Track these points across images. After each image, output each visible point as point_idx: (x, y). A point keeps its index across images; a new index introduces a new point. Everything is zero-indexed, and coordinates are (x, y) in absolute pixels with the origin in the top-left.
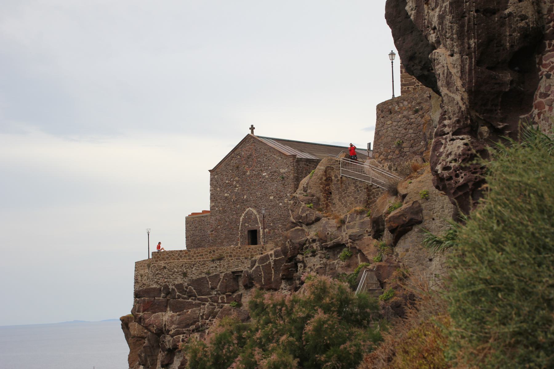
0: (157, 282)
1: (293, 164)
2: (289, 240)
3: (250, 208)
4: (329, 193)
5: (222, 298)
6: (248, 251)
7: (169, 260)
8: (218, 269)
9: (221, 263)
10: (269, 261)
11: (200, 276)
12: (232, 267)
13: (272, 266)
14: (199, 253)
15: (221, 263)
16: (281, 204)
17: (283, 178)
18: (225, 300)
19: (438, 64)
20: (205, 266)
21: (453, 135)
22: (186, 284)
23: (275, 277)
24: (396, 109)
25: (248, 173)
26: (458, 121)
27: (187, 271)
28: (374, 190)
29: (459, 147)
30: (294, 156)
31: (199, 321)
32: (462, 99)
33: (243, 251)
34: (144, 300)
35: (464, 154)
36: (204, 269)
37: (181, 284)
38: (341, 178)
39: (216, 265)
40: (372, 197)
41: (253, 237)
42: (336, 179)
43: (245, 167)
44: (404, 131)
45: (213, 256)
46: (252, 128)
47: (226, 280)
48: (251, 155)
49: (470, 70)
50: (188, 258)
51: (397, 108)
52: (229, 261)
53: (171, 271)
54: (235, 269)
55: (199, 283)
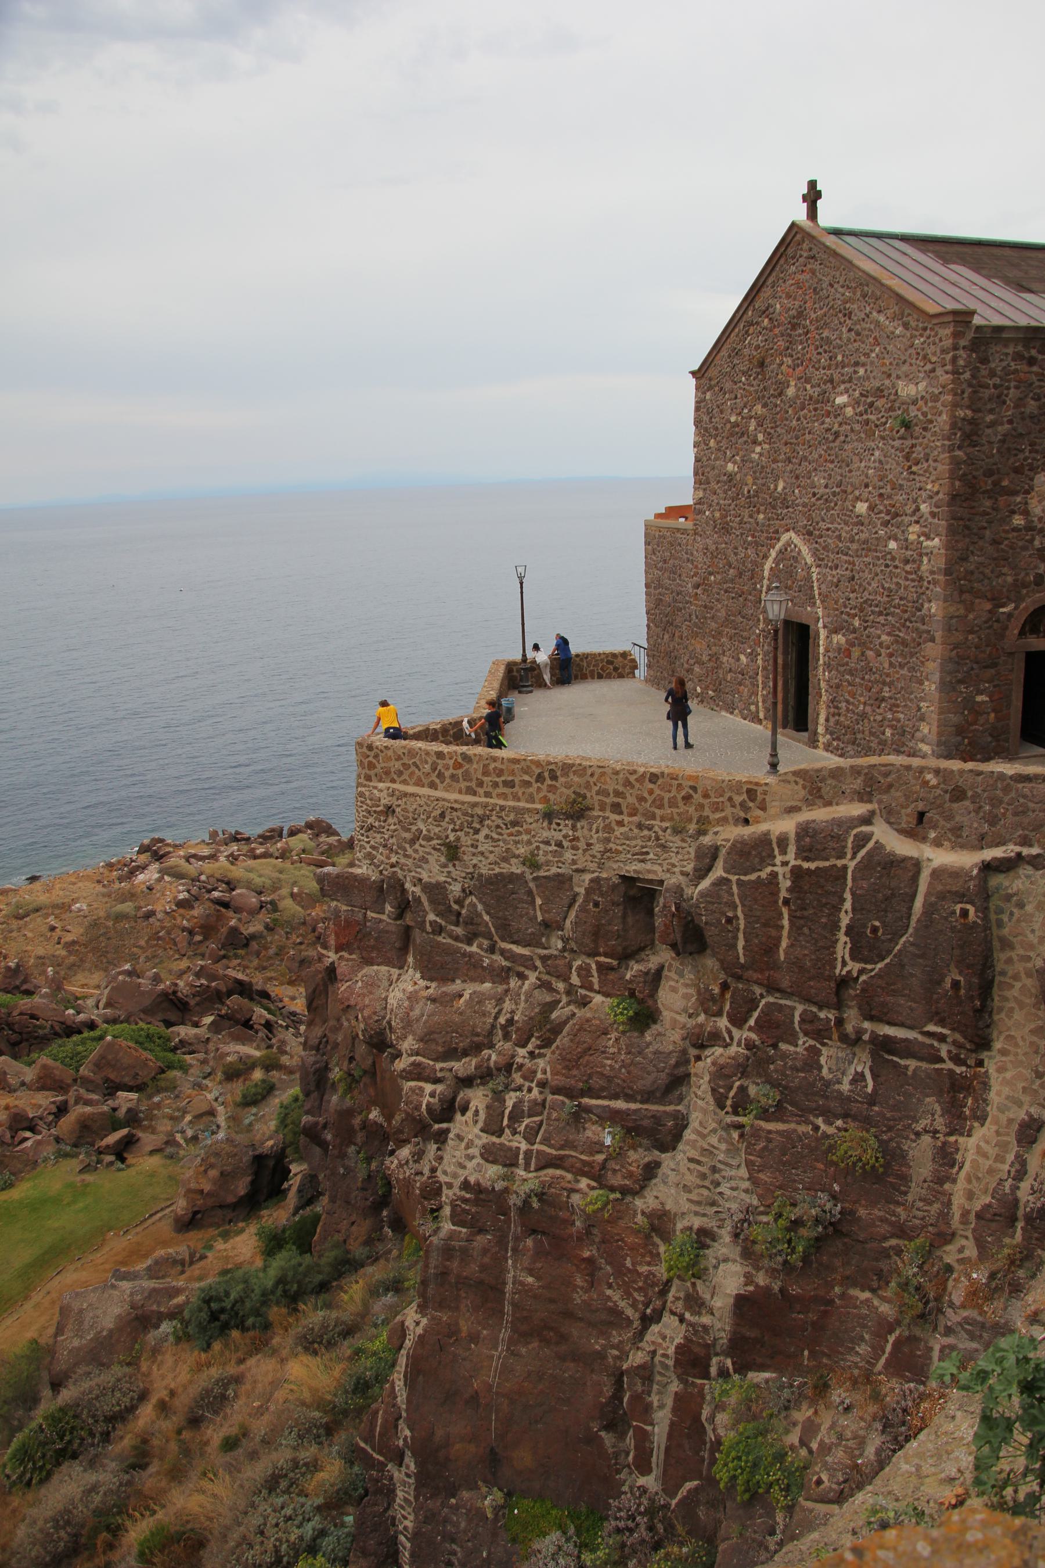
1: (954, 359)
5: (584, 972)
6: (687, 798)
7: (404, 782)
8: (568, 855)
9: (578, 834)
10: (769, 869)
11: (505, 868)
13: (783, 894)
14: (500, 773)
17: (907, 425)
20: (519, 833)
22: (456, 889)
23: (791, 946)
25: (791, 392)
27: (458, 839)
30: (962, 318)
31: (491, 1046)
33: (667, 796)
36: (516, 842)
39: (558, 836)
45: (550, 796)
46: (813, 196)
47: (596, 904)
48: (800, 314)
50: (463, 785)
52: (608, 829)
53: (408, 830)
54: (632, 868)
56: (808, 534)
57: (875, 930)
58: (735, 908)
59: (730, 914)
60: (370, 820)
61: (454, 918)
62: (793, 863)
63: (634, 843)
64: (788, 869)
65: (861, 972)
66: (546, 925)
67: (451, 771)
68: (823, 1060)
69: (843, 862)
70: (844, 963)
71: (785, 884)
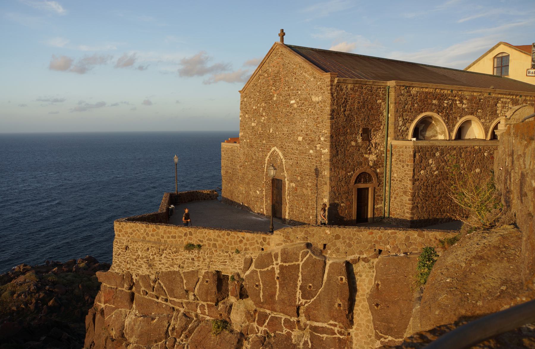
8: (196, 264)
9: (200, 255)
10: (271, 267)
11: (172, 269)
13: (277, 275)
15: (200, 255)
16: (311, 151)
22: (153, 277)
23: (280, 295)
25: (275, 99)
27: (154, 258)
33: (233, 240)
39: (193, 256)
43: (271, 89)
46: (282, 34)
47: (207, 282)
48: (278, 72)
56: (281, 148)
57: (310, 287)
58: (259, 281)
59: (257, 284)
60: (120, 251)
61: (152, 289)
62: (280, 264)
63: (221, 258)
65: (306, 303)
66: (187, 291)
68: (292, 337)
69: (298, 263)
70: (299, 300)
71: (277, 271)
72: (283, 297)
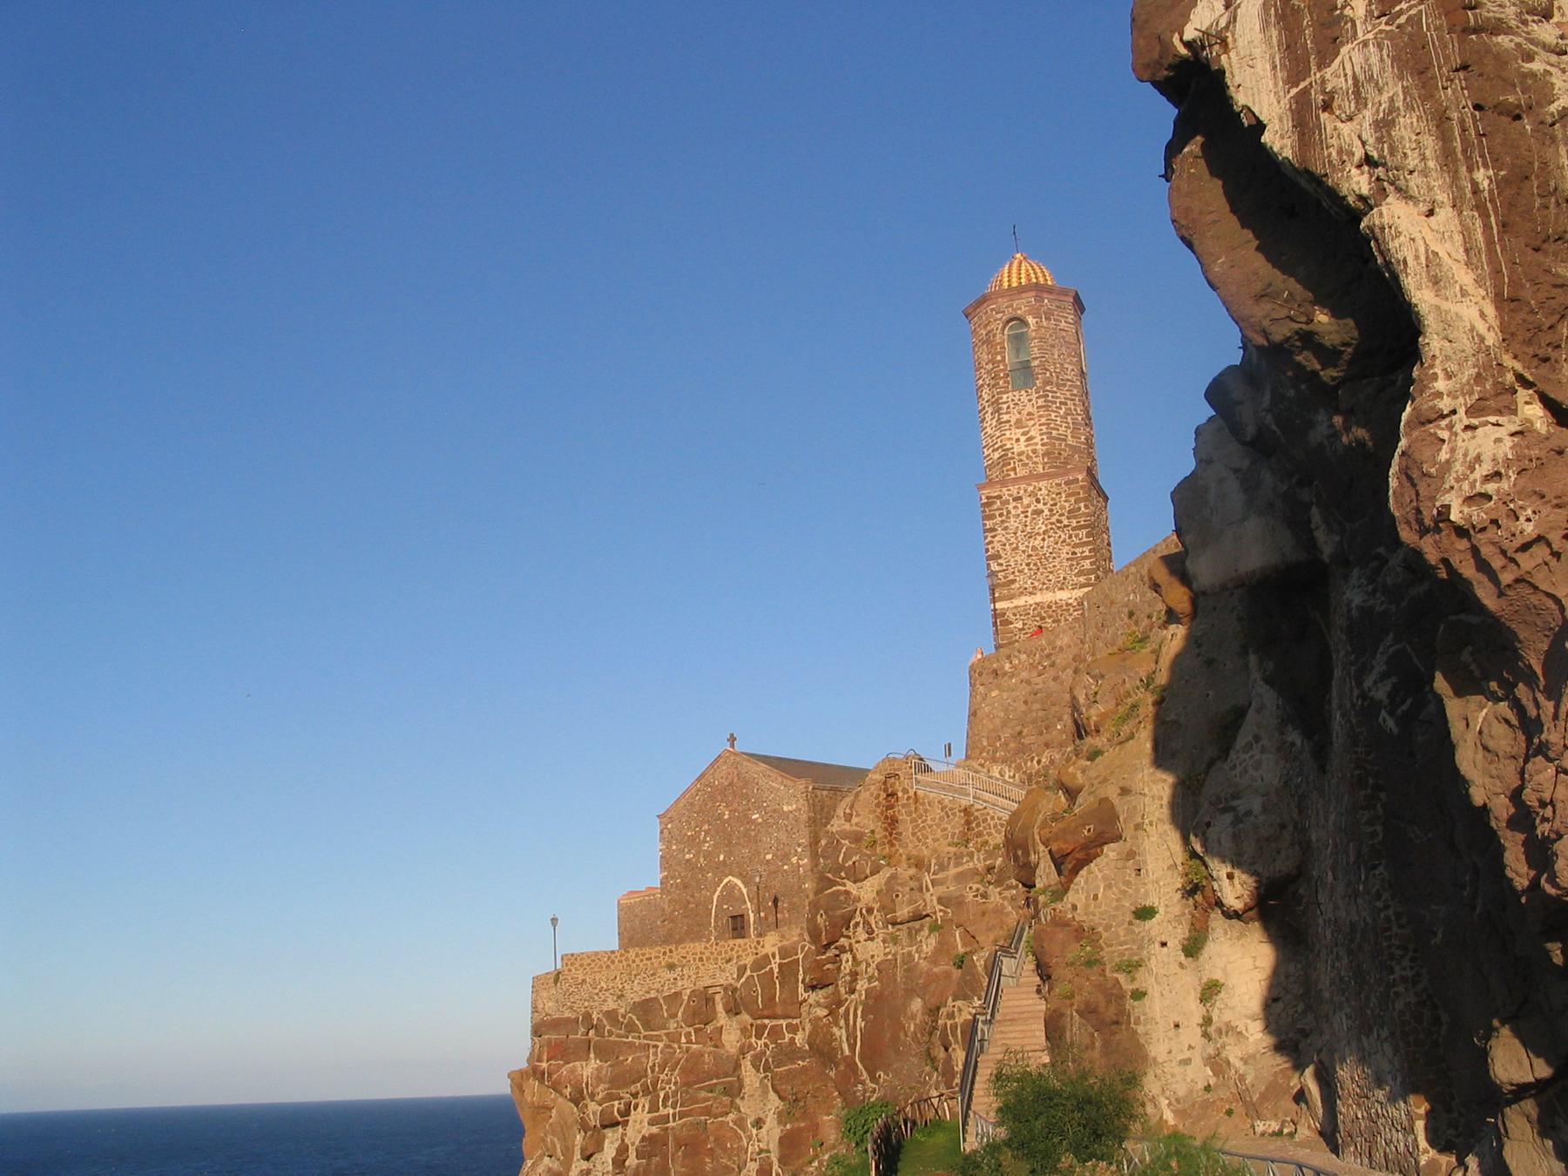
0: (571, 1008)
2: (822, 912)
3: (730, 877)
4: (892, 823)
8: (680, 983)
10: (769, 967)
11: (648, 996)
12: (704, 979)
14: (643, 955)
16: (786, 867)
18: (693, 1038)
19: (1398, 234)
21: (1470, 412)
23: (780, 994)
24: (1007, 668)
25: (726, 817)
26: (1479, 378)
28: (976, 814)
29: (1498, 440)
32: (1482, 315)
33: (723, 950)
34: (550, 1039)
35: (1519, 458)
37: (615, 1011)
38: (915, 793)
40: (974, 825)
41: (738, 925)
42: (906, 796)
43: (720, 805)
44: (1023, 708)
46: (732, 739)
47: (694, 1001)
49: (1490, 242)
51: (1007, 666)
55: (646, 1009)
56: (740, 876)
64: (777, 965)
67: (619, 958)
68: (796, 1041)
71: (776, 970)
72: (784, 996)
